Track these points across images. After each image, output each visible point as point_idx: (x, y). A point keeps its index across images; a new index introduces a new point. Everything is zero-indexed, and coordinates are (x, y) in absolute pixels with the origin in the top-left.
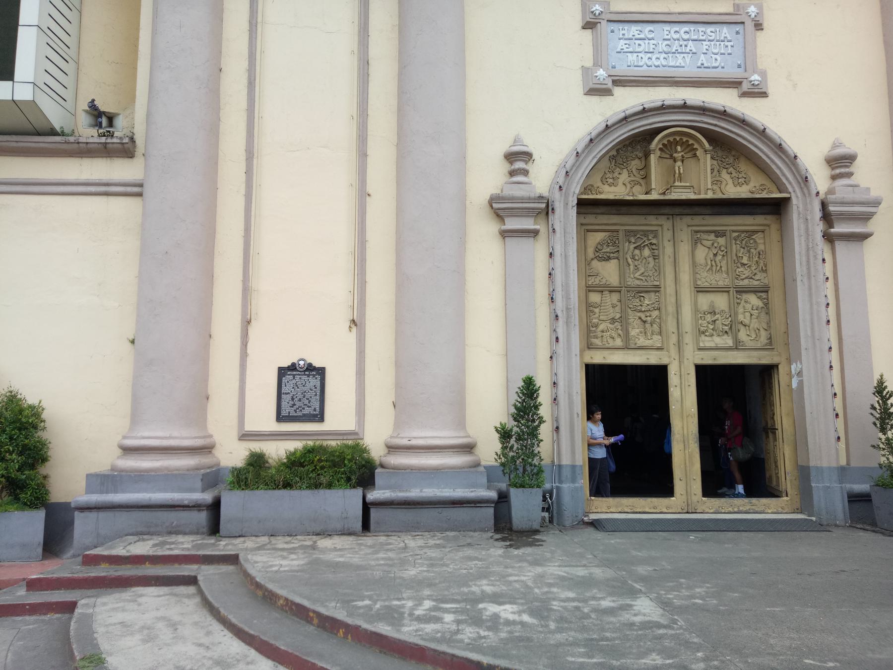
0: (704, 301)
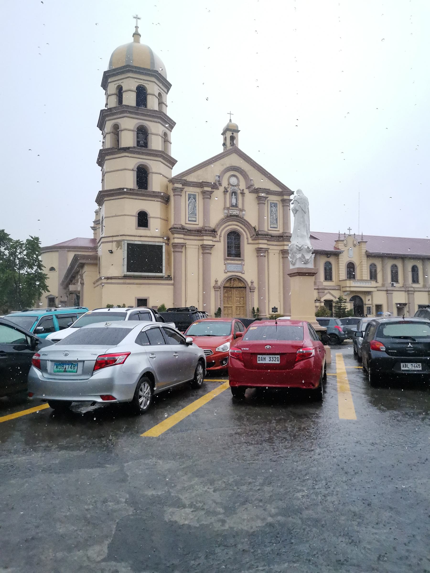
0: (237, 298)
